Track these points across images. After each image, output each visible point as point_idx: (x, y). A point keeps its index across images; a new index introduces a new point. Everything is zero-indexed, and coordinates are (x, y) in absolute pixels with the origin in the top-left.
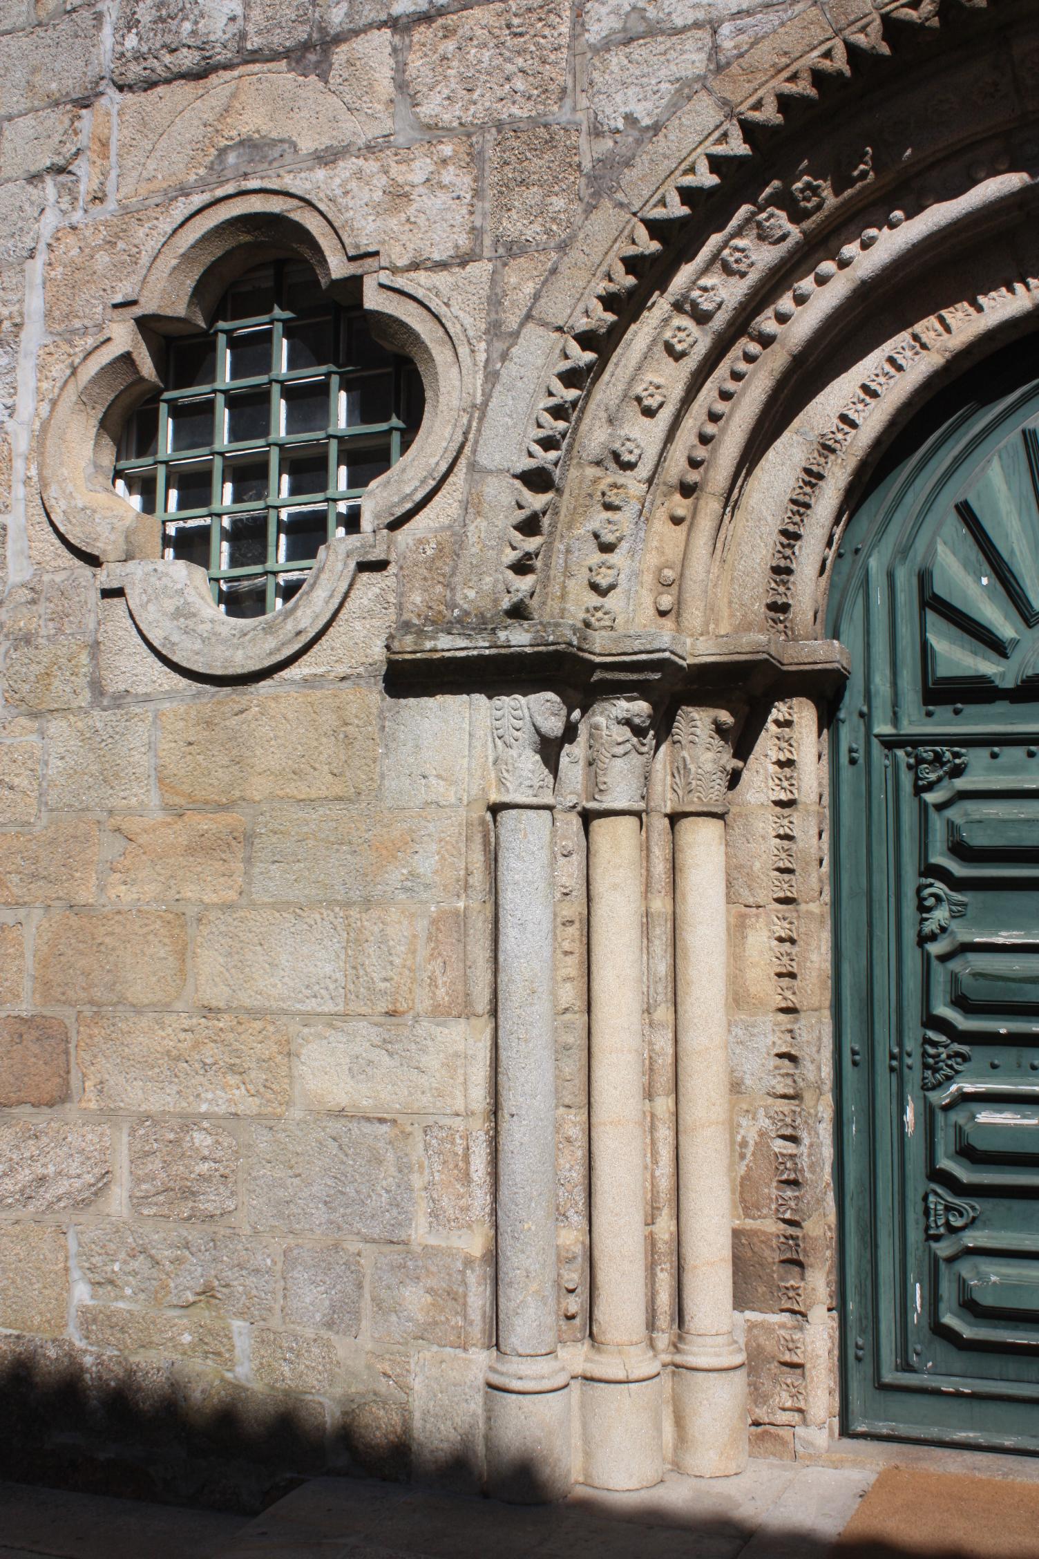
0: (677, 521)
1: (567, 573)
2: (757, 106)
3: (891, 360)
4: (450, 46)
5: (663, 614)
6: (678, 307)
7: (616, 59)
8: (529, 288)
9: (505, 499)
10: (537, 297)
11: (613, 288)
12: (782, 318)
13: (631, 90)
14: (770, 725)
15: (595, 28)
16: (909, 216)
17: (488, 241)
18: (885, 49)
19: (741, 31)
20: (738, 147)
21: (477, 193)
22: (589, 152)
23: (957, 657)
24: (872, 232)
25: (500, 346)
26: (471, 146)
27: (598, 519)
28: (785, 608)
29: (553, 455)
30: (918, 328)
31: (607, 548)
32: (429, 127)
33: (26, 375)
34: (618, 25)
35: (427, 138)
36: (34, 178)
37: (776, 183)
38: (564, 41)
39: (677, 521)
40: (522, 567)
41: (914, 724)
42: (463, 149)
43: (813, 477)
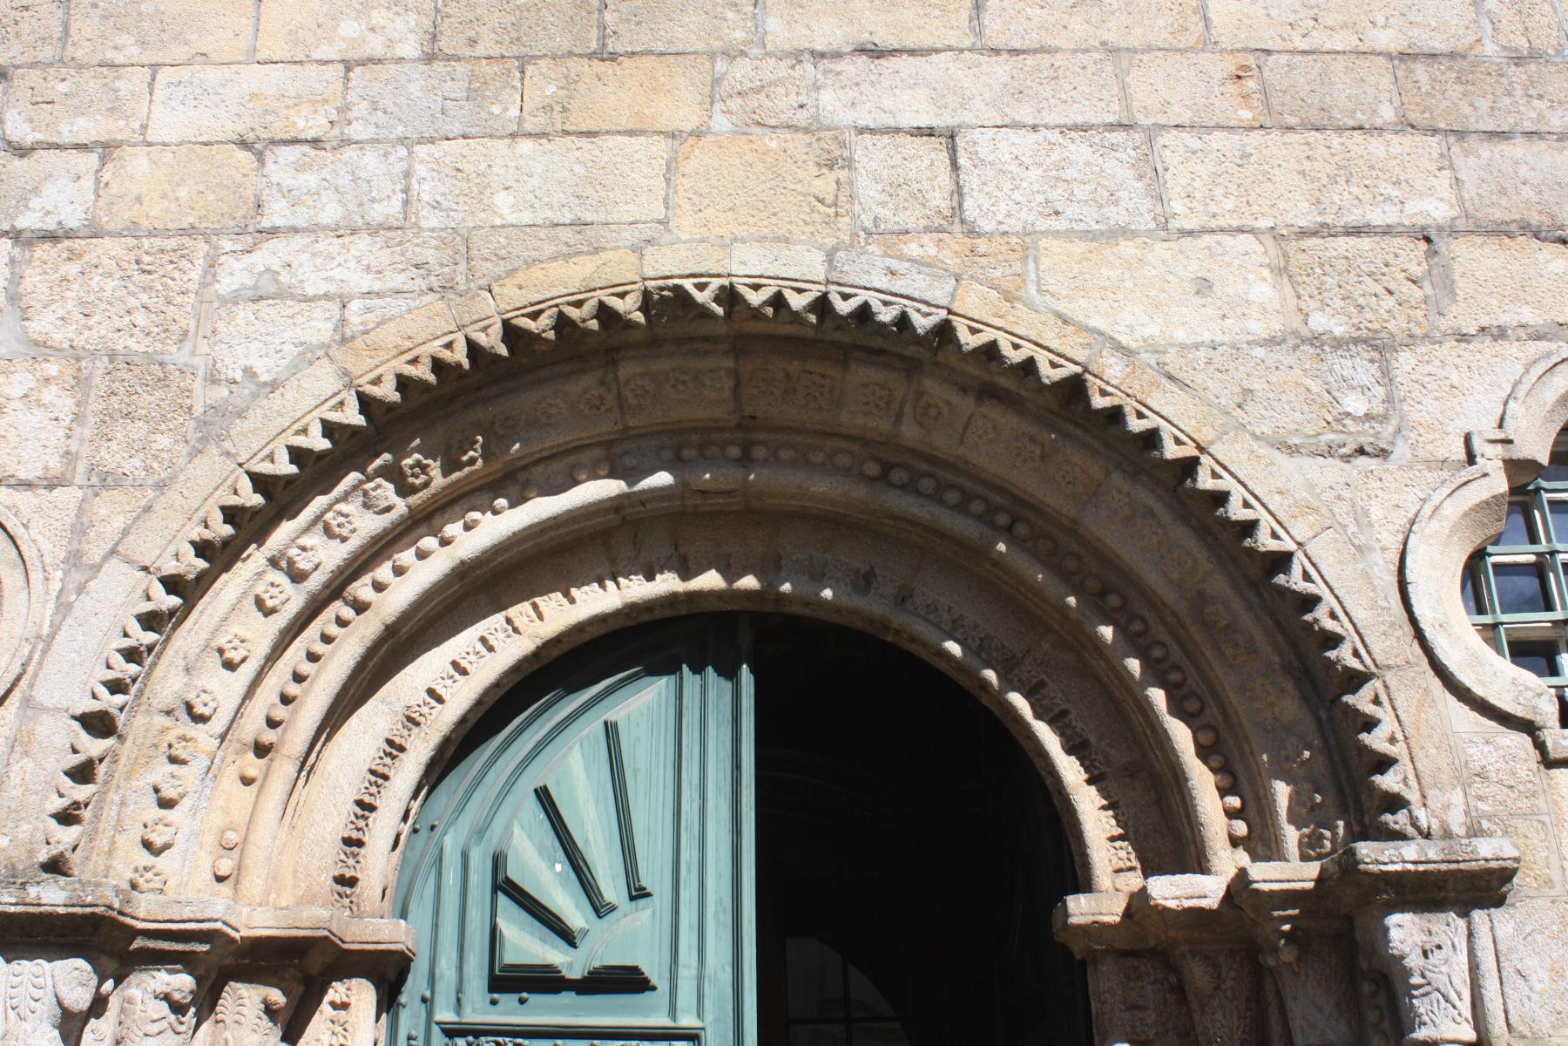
0: (247, 781)
1: (119, 828)
2: (377, 381)
3: (483, 640)
4: (73, 269)
5: (220, 879)
6: (273, 562)
7: (243, 313)
8: (119, 522)
9: (61, 740)
10: (125, 532)
11: (208, 535)
12: (379, 587)
13: (254, 344)
14: (325, 1006)
15: (226, 280)
16: (512, 506)
17: (81, 467)
18: (503, 350)
19: (369, 310)
20: (352, 416)
21: (77, 418)
22: (202, 397)
23: (526, 944)
24: (475, 515)
25: (77, 577)
26: (79, 370)
27: (161, 772)
28: (351, 882)
29: (119, 699)
30: (512, 612)
31: (166, 804)
32: (36, 343)
34: (250, 283)
35: (33, 354)
37: (387, 456)
38: (193, 287)
39: (247, 781)
40: (67, 817)
41: (479, 1011)
42: (70, 371)
43: (395, 748)
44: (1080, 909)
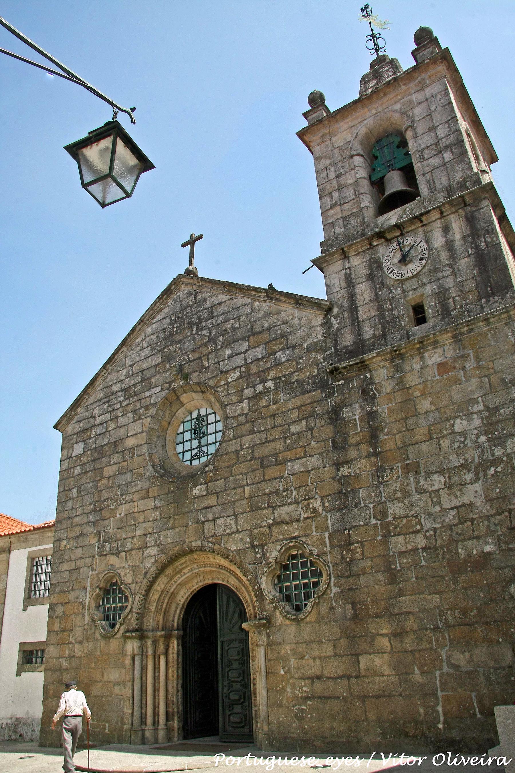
20: (157, 571)
40: (137, 624)
43: (177, 608)
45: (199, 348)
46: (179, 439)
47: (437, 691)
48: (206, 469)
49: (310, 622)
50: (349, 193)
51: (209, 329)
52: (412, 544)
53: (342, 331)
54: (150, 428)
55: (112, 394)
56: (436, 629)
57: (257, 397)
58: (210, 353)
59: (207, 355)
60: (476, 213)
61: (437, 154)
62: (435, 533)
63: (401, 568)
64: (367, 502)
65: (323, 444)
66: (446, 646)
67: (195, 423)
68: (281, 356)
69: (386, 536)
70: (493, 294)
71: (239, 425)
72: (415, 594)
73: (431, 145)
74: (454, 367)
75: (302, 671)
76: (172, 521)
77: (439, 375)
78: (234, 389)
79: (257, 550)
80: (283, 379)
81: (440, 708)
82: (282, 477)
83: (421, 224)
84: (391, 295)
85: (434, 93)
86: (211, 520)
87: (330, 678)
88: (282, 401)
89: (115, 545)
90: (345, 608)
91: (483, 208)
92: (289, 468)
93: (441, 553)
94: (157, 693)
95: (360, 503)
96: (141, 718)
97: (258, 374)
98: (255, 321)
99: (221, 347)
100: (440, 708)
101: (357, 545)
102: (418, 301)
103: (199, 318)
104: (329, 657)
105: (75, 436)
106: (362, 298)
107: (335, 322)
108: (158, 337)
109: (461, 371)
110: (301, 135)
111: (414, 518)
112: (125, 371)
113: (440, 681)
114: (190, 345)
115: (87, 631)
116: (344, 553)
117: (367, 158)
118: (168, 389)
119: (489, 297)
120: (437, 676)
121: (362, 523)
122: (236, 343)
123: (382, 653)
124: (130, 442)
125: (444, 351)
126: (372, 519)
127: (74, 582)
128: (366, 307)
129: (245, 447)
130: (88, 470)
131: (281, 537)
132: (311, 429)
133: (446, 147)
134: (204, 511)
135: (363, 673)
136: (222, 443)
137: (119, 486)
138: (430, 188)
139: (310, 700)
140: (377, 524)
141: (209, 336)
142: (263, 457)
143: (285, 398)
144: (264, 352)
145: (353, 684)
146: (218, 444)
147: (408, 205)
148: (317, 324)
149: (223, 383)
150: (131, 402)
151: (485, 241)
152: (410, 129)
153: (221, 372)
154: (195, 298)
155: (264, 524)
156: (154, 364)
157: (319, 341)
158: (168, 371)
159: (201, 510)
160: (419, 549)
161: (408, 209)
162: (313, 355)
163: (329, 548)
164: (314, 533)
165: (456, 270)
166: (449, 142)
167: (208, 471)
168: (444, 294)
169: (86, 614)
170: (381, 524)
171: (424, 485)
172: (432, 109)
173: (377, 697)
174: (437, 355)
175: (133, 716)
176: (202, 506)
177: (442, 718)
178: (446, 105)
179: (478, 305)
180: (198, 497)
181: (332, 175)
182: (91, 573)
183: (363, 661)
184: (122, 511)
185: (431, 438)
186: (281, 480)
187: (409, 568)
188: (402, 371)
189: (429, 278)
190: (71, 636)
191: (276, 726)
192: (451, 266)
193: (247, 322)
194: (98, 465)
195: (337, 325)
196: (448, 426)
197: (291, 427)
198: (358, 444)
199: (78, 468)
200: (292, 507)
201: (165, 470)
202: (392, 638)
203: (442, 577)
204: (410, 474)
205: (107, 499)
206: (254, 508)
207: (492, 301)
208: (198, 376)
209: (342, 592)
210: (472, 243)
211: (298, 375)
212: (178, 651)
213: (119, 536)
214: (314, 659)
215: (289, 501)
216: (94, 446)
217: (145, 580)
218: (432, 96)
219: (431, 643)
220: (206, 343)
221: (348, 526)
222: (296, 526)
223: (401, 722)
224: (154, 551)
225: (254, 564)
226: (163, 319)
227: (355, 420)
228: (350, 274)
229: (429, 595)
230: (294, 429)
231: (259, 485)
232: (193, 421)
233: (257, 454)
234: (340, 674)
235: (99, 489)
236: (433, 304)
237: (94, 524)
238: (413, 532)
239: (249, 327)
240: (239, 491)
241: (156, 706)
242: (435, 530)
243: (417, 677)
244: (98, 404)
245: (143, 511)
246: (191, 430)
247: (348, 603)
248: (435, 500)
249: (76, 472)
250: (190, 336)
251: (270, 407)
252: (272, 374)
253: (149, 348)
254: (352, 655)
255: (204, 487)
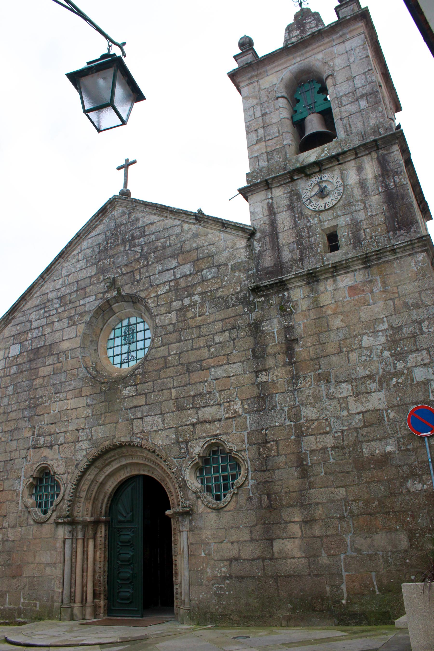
33: (21, 483)
36: (23, 458)
40: (68, 511)
44: (168, 512)
45: (131, 263)
46: (111, 344)
47: (342, 571)
48: (136, 372)
49: (229, 511)
50: (274, 130)
51: (141, 246)
52: (322, 443)
53: (264, 253)
54: (84, 333)
55: (49, 301)
56: (342, 518)
57: (183, 310)
58: (141, 268)
59: (139, 270)
60: (386, 156)
61: (353, 102)
62: (343, 434)
63: (312, 464)
64: (283, 405)
65: (244, 353)
66: (350, 532)
67: (125, 330)
68: (208, 274)
69: (300, 435)
70: (400, 228)
71: (167, 334)
72: (324, 487)
73: (349, 93)
74: (363, 290)
75: (221, 553)
76: (103, 418)
77: (350, 296)
78: (163, 301)
79: (182, 446)
80: (209, 294)
81: (344, 587)
82: (206, 381)
83: (338, 163)
84: (308, 224)
85: (353, 47)
86: (140, 418)
87: (247, 560)
88: (207, 314)
89: (49, 438)
90: (261, 498)
91: (393, 152)
92: (213, 373)
93: (347, 452)
94: (85, 574)
95: (276, 406)
96: (71, 596)
97: (186, 288)
98: (185, 241)
99: (152, 263)
100: (344, 587)
101: (272, 443)
102: (332, 230)
103: (132, 235)
104: (246, 541)
105: (12, 338)
106: (282, 225)
107: (257, 246)
108: (93, 251)
109: (369, 294)
110: (233, 76)
111: (324, 421)
112: (61, 280)
113: (345, 563)
114: (123, 260)
115: (20, 517)
116: (261, 450)
117: (290, 101)
118: (101, 299)
119: (396, 230)
120: (342, 558)
121: (277, 424)
122: (166, 260)
123: (293, 538)
124: (65, 346)
125: (355, 275)
126: (287, 420)
127: (9, 471)
128: (286, 233)
129: (172, 353)
130: (24, 369)
131: (204, 434)
132: (234, 340)
133: (362, 96)
134: (133, 410)
135: (276, 555)
136: (152, 349)
137: (54, 385)
138: (346, 131)
139: (228, 579)
140: (291, 425)
141: (141, 253)
142: (189, 363)
143: (210, 311)
144: (192, 269)
145: (267, 565)
146: (146, 350)
147: (326, 145)
148: (241, 247)
149: (153, 295)
150: (66, 309)
151: (394, 182)
152: (330, 77)
153: (152, 286)
154: (129, 218)
155: (188, 423)
156: (89, 275)
157: (242, 261)
158: (101, 282)
159: (130, 408)
160: (327, 448)
161: (326, 149)
162: (237, 274)
163: (247, 446)
164: (234, 432)
165: (367, 206)
166: (365, 91)
167: (138, 374)
168: (356, 225)
169: (20, 501)
170: (294, 425)
171: (333, 392)
172: (352, 60)
173: (289, 577)
174: (348, 279)
175: (63, 595)
176: (131, 405)
177: (345, 595)
178: (363, 58)
179: (386, 237)
180: (128, 397)
181: (258, 114)
182: (25, 464)
183: (277, 546)
184: (56, 407)
185: (341, 352)
186: (204, 384)
187: (319, 464)
188: (317, 292)
189: (343, 211)
190: (5, 522)
191: (197, 602)
192: (363, 201)
193: (177, 242)
194: (34, 366)
195: (259, 248)
196: (356, 342)
197: (215, 337)
198: (275, 354)
199: (15, 367)
200: (215, 408)
201: (97, 371)
202: (303, 525)
203: (348, 472)
204: (322, 382)
205: (41, 397)
206: (180, 408)
207: (398, 235)
208: (131, 288)
209: (258, 484)
210: (382, 182)
211: (223, 291)
212: (105, 536)
213: (52, 431)
214: (232, 543)
215: (212, 403)
216: (30, 348)
217: (77, 471)
218: (352, 49)
219: (337, 529)
220: (138, 258)
221: (265, 427)
222: (218, 426)
223: (310, 598)
224: (85, 445)
225: (179, 458)
226: (98, 235)
227: (273, 333)
228: (272, 203)
229: (336, 488)
230: (217, 339)
231: (185, 388)
232: (123, 329)
233: (183, 361)
234: (256, 556)
235: (34, 387)
236: (346, 233)
237: (29, 419)
238: (324, 433)
239: (178, 245)
240: (166, 392)
241: (84, 585)
242: (343, 431)
243: (324, 559)
244: (35, 309)
245: (76, 409)
246: (121, 336)
247: (263, 494)
248: (343, 405)
249: (12, 372)
250: (123, 251)
251: (196, 319)
252: (199, 289)
253: (85, 261)
254: (267, 539)
255: (133, 388)
